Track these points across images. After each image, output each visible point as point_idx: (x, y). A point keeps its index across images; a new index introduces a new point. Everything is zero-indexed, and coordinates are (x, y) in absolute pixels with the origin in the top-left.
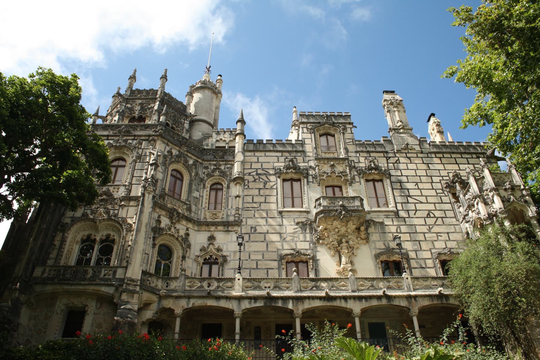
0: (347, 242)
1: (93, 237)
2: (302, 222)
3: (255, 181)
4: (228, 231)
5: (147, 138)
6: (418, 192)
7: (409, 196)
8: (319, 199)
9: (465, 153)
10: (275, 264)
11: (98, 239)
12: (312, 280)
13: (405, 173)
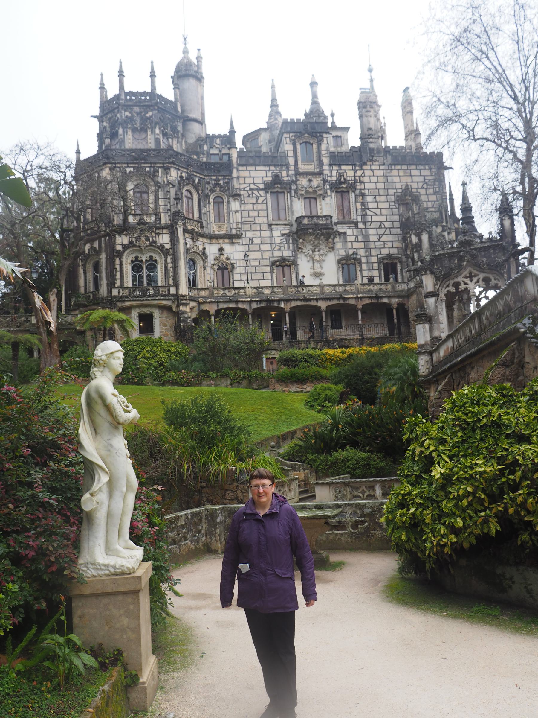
0: (319, 251)
1: (140, 259)
3: (249, 196)
4: (233, 243)
5: (162, 165)
6: (374, 205)
7: (368, 209)
8: (300, 217)
9: (420, 164)
10: (268, 269)
11: (144, 261)
12: (295, 287)
13: (367, 186)
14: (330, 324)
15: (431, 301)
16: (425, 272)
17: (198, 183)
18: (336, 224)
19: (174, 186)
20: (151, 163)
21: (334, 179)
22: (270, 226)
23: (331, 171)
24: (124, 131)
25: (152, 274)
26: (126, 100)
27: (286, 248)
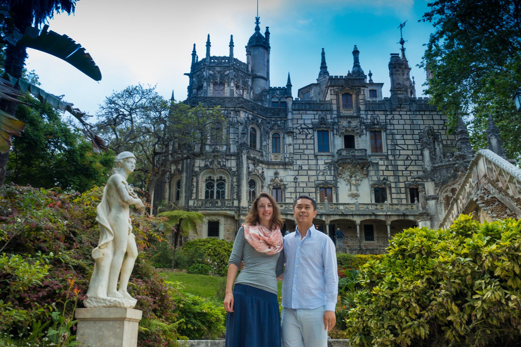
0: (355, 177)
1: (212, 178)
2: (329, 163)
3: (300, 133)
5: (233, 109)
6: (402, 142)
7: (397, 145)
8: (341, 150)
10: (313, 190)
11: (215, 180)
12: (335, 204)
13: (396, 127)
14: (363, 235)
15: (432, 203)
16: (427, 180)
17: (261, 123)
18: (370, 156)
19: (242, 124)
20: (226, 107)
21: (369, 121)
22: (316, 156)
23: (367, 115)
24: (207, 84)
25: (221, 190)
26: (211, 62)
27: (329, 174)
